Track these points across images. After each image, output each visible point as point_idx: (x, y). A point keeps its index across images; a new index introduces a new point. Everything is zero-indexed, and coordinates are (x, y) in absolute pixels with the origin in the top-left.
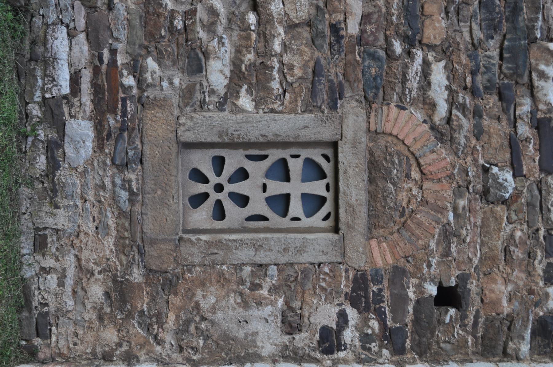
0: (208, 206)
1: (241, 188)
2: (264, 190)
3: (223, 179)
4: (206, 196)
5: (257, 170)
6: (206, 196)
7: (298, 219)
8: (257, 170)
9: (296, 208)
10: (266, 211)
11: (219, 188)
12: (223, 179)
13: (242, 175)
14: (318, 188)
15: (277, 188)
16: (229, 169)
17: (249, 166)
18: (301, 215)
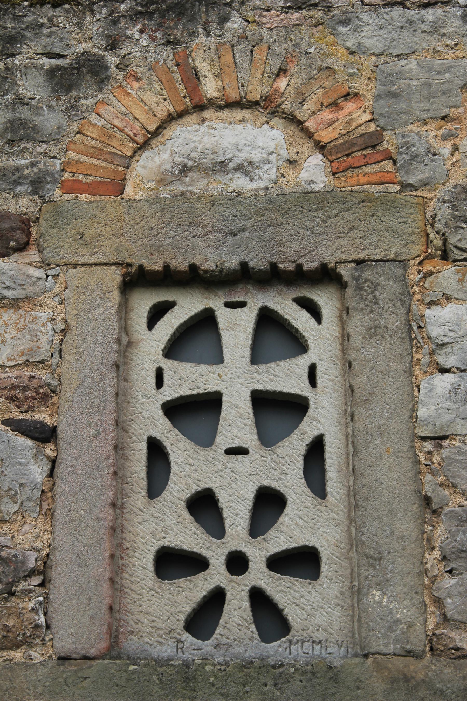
0: (285, 591)
1: (237, 510)
2: (240, 451)
3: (216, 554)
4: (258, 598)
5: (191, 467)
6: (258, 598)
7: (312, 370)
8: (191, 467)
9: (285, 377)
10: (294, 446)
11: (237, 563)
12: (216, 554)
13: (204, 505)
14: (237, 328)
15: (237, 421)
16: (188, 536)
17: (180, 487)
18: (301, 363)
